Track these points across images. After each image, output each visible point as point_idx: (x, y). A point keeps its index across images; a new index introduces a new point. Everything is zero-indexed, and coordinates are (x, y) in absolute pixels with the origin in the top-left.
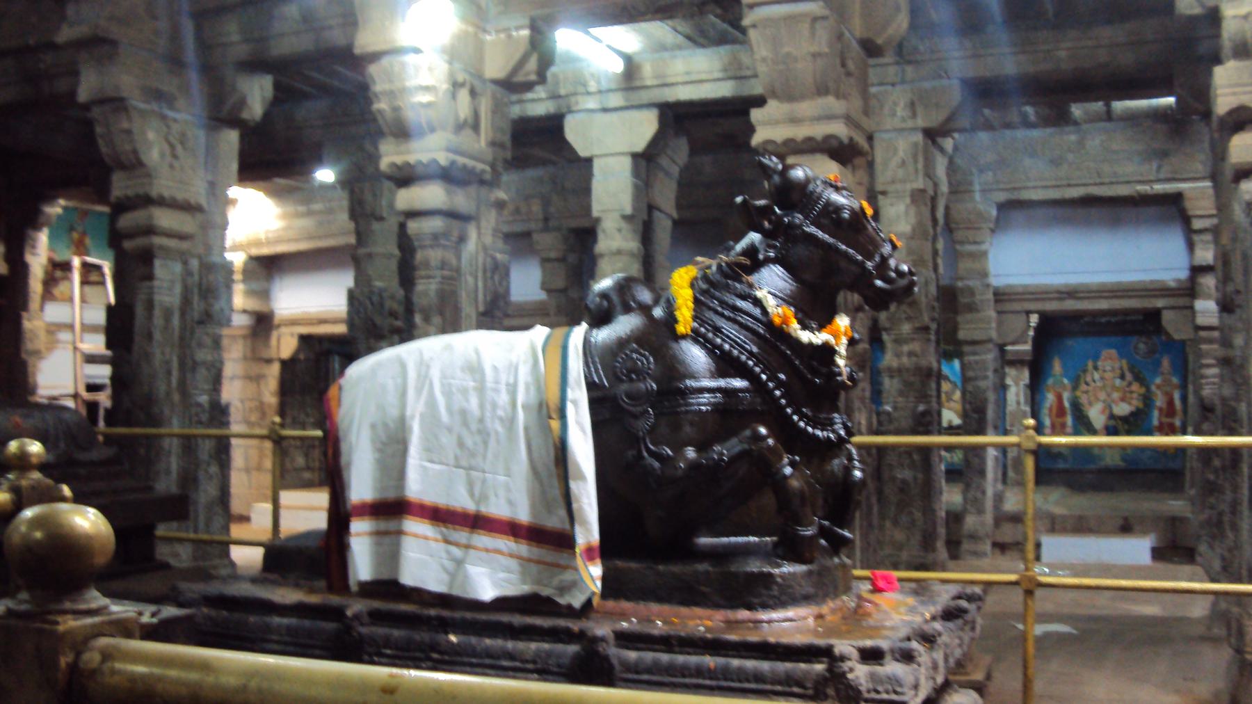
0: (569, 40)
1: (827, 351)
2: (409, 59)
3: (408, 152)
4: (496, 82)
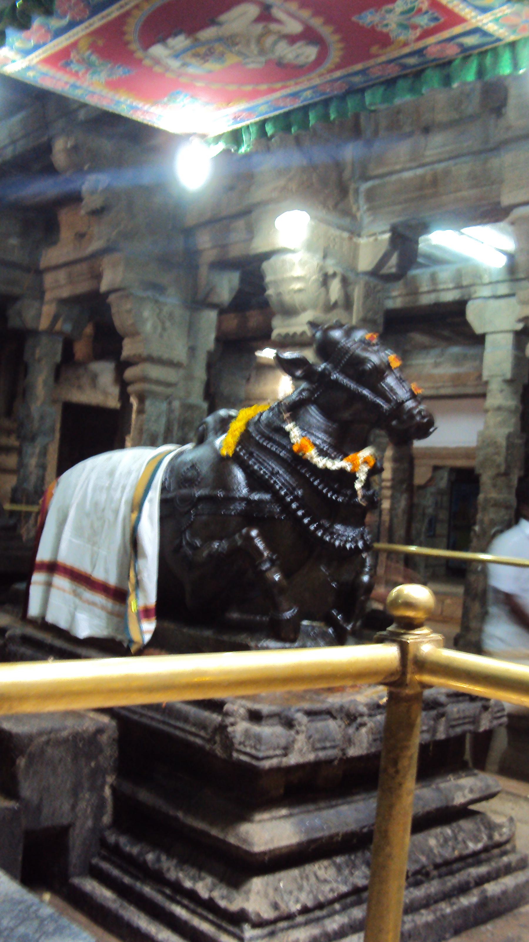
0: (444, 240)
1: (346, 478)
2: (288, 257)
3: (289, 326)
4: (366, 273)
